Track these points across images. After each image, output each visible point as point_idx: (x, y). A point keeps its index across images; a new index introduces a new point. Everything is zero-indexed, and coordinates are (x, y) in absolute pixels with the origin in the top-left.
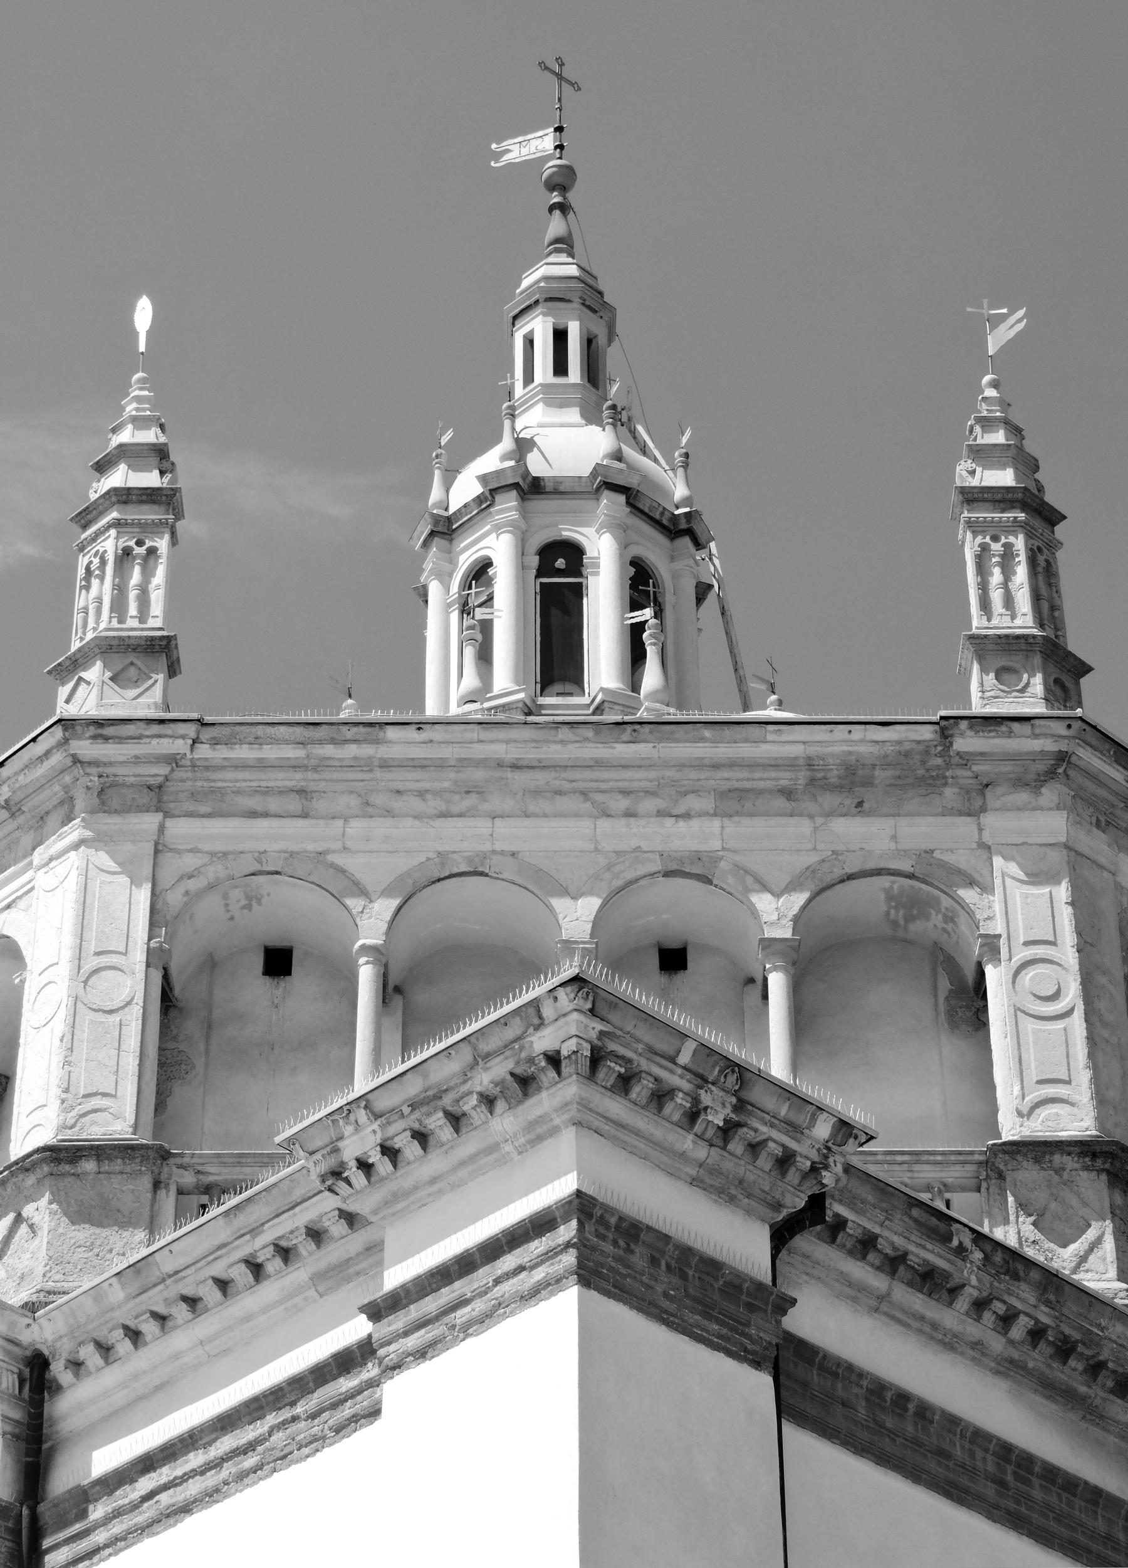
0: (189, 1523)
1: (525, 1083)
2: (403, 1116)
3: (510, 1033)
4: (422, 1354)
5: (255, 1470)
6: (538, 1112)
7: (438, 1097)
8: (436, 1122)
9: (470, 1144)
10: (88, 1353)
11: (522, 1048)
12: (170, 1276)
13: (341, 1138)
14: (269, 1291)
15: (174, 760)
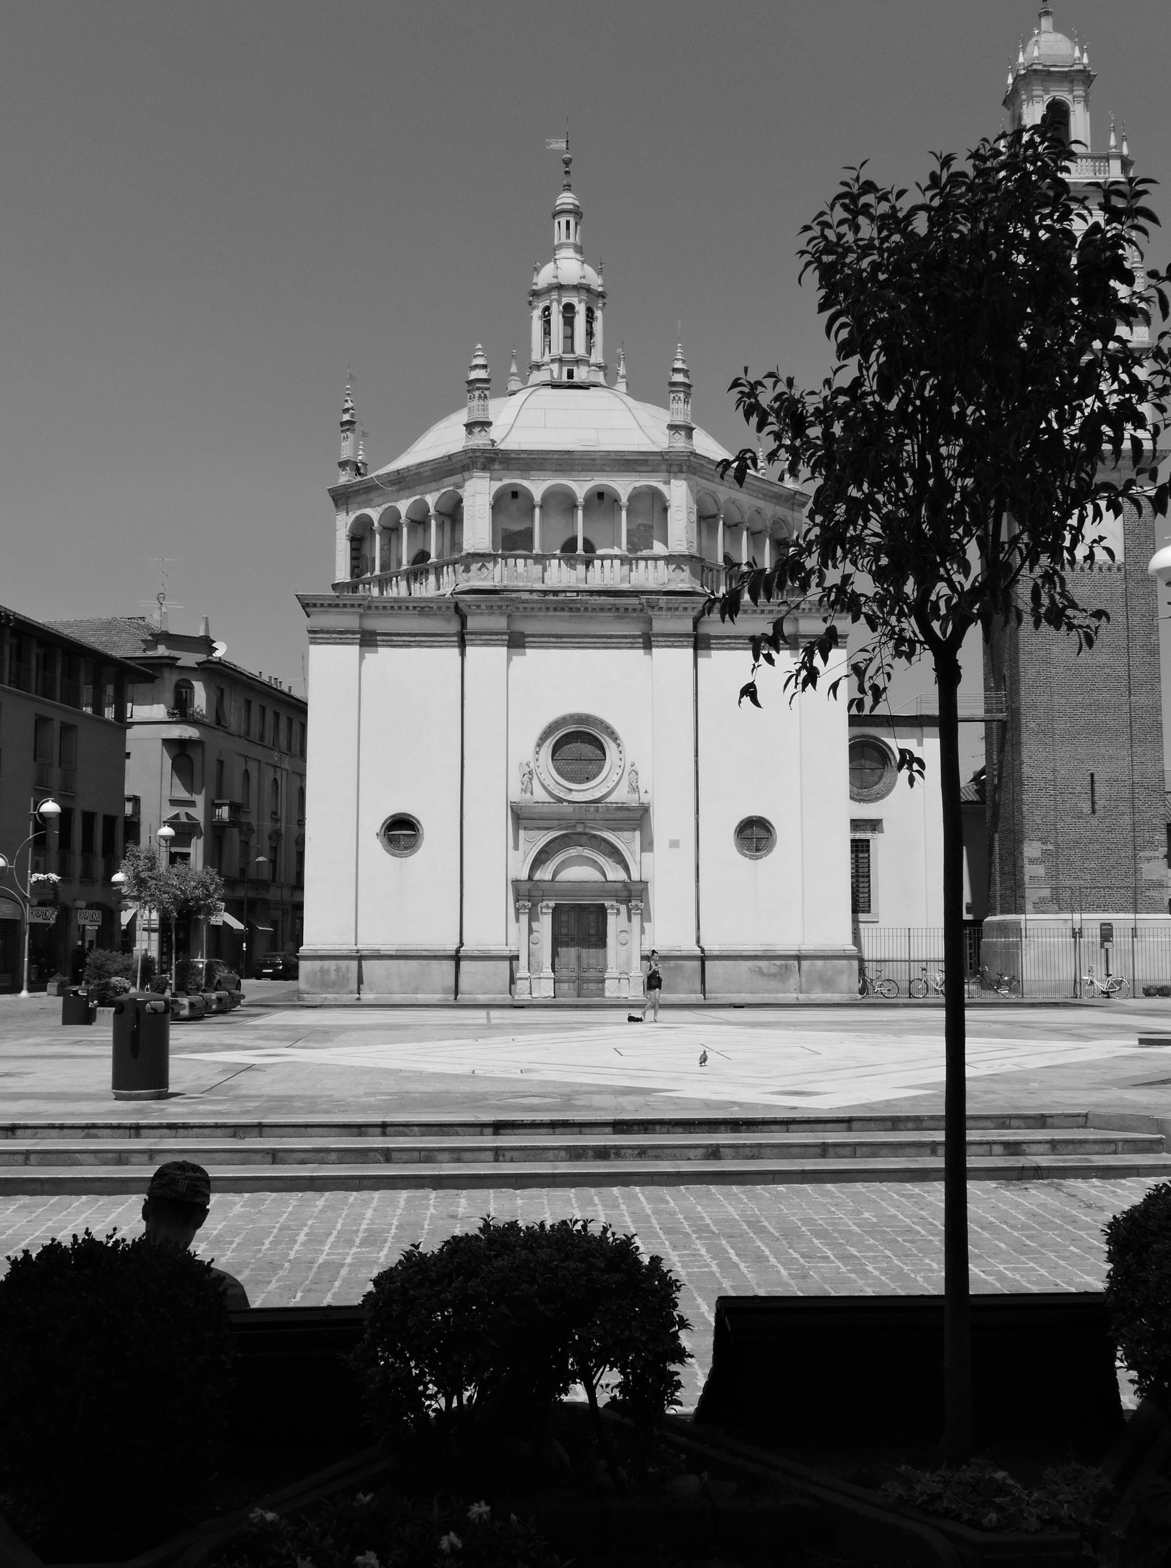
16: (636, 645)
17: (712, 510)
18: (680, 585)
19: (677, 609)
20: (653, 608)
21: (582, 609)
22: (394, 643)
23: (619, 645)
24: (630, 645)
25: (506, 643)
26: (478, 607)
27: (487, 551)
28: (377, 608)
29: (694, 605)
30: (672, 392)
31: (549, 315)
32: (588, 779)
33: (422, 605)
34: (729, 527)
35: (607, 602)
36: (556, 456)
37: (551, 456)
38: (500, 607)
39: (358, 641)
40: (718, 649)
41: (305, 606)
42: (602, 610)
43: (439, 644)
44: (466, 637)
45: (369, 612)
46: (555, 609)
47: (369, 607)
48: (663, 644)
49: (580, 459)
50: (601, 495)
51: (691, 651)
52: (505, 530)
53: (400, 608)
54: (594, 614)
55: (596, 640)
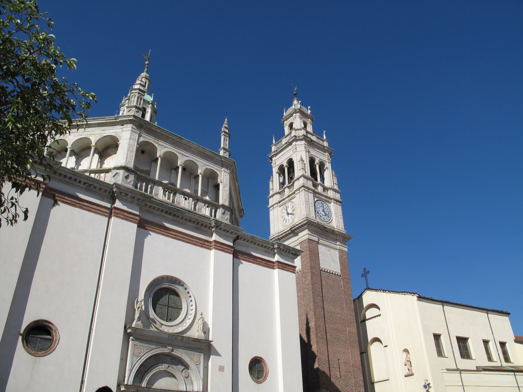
5: (258, 264)
14: (261, 248)
16: (204, 246)
19: (228, 231)
20: (217, 227)
24: (201, 245)
25: (137, 222)
26: (127, 195)
28: (60, 174)
29: (236, 232)
32: (171, 320)
33: (90, 183)
35: (194, 217)
36: (174, 138)
37: (172, 137)
42: (190, 221)
46: (166, 212)
49: (185, 145)
51: (232, 256)
53: (75, 180)
55: (184, 236)
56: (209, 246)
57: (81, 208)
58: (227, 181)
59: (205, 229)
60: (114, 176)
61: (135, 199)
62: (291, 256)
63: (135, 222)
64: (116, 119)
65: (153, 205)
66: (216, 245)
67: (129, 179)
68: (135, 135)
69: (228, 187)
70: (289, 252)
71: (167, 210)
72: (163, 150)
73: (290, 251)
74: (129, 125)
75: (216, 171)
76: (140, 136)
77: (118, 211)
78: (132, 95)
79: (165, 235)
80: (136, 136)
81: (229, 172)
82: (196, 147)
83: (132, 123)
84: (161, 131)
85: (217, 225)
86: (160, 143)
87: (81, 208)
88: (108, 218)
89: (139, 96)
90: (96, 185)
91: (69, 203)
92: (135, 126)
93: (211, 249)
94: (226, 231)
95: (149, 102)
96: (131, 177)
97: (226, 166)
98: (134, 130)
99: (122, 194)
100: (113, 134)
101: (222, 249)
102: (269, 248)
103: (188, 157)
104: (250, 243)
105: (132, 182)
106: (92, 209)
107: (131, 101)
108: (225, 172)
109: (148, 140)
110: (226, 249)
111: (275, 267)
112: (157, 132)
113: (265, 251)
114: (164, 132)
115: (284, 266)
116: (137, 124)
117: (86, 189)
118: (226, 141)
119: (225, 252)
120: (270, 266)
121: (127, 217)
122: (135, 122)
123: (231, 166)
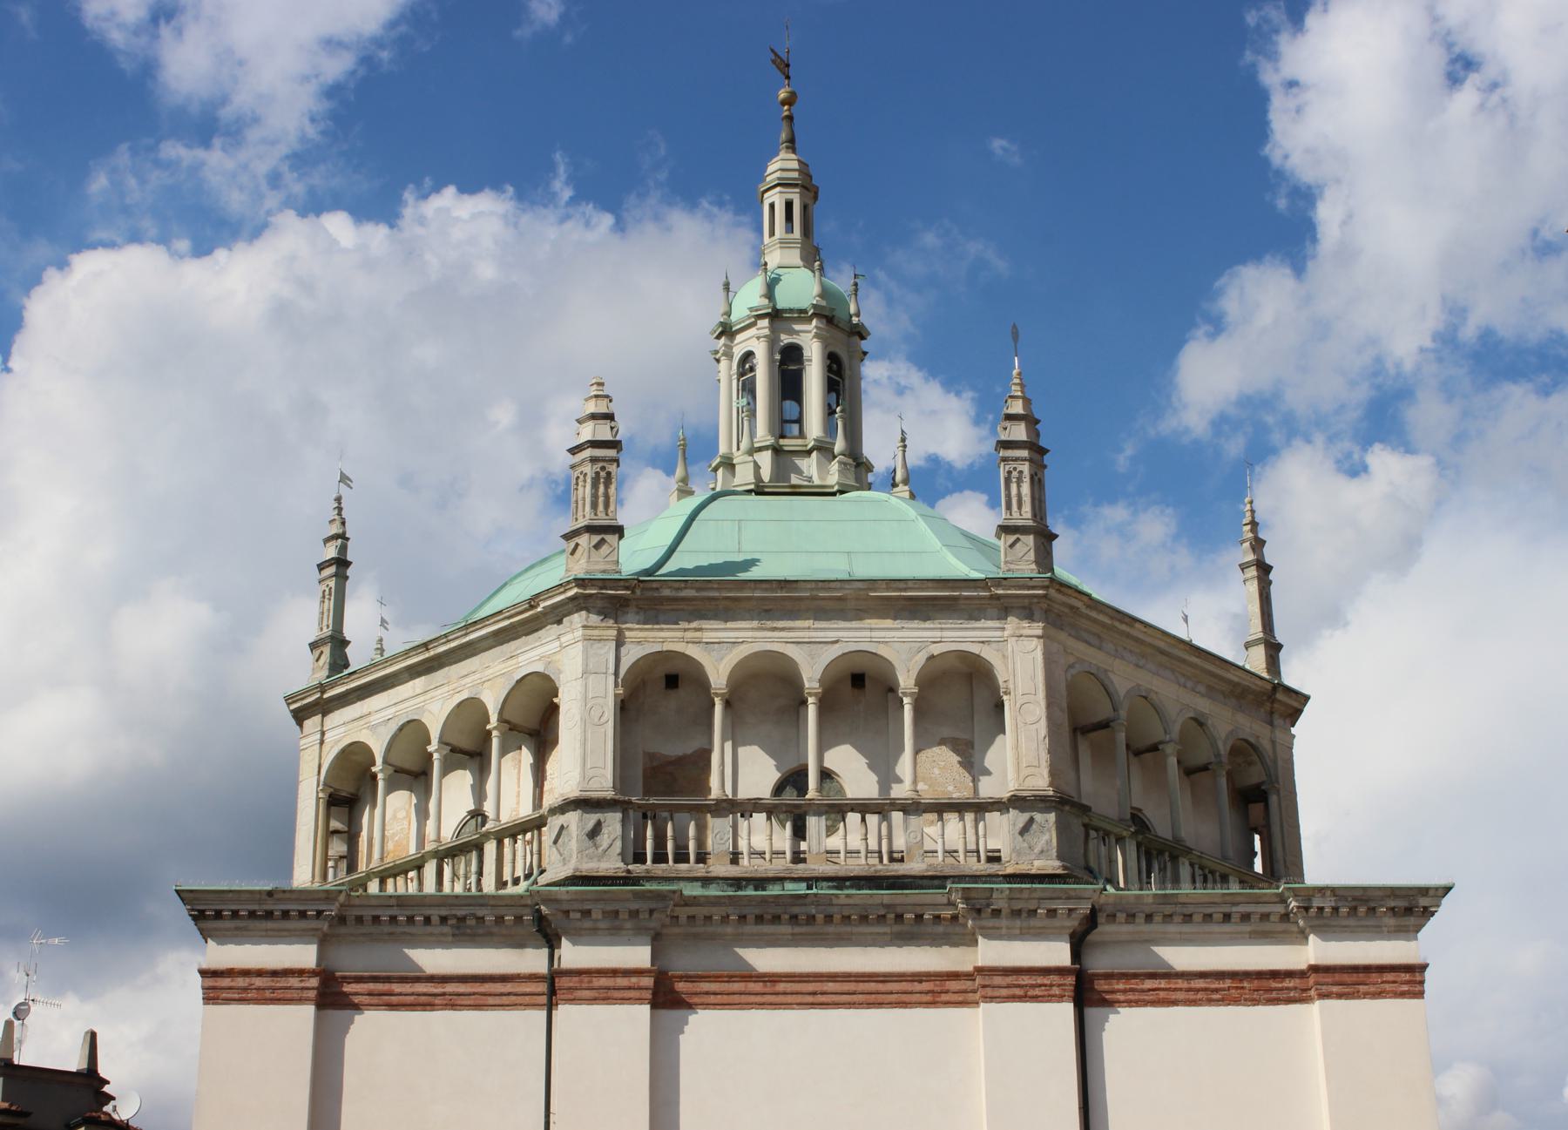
0: (1175, 1009)
1: (1409, 911)
2: (1347, 900)
3: (1411, 893)
4: (1340, 996)
5: (1218, 1000)
6: (1407, 923)
7: (1367, 901)
8: (1362, 910)
9: (1371, 922)
10: (1121, 917)
11: (1414, 899)
12: (1181, 904)
13: (1313, 896)
14: (1227, 928)
15: (1072, 607)
16: (944, 997)
17: (1103, 711)
18: (1037, 863)
20: (979, 911)
21: (820, 917)
22: (394, 999)
23: (905, 998)
24: (928, 998)
25: (648, 995)
27: (610, 794)
30: (1004, 459)
31: (752, 369)
33: (460, 912)
34: (1138, 753)
38: (634, 914)
39: (312, 994)
40: (1130, 1003)
41: (199, 917)
42: (864, 919)
43: (497, 1000)
44: (562, 982)
45: (343, 930)
46: (760, 919)
47: (342, 919)
48: (1004, 992)
50: (858, 680)
51: (1068, 1008)
52: (651, 756)
54: (848, 929)
56: (965, 992)
57: (453, 1005)
58: (1034, 678)
59: (940, 929)
60: (555, 842)
61: (621, 916)
62: (1390, 921)
63: (639, 1001)
64: (532, 607)
65: (700, 912)
66: (987, 983)
67: (606, 836)
68: (602, 652)
69: (1043, 704)
70: (1372, 910)
71: (758, 911)
72: (725, 661)
73: (1372, 905)
74: (576, 615)
75: (974, 649)
76: (620, 642)
77: (570, 981)
78: (576, 476)
79: (771, 1004)
80: (608, 652)
81: (1039, 632)
82: (860, 589)
83: (583, 605)
84: (698, 590)
85: (978, 907)
86: (708, 636)
87: (453, 1005)
88: (543, 1014)
89: (597, 474)
90: (480, 913)
91: (409, 1002)
92: (599, 613)
93: (977, 1003)
94: (1024, 915)
95: (804, 311)
96: (610, 828)
97: (1024, 608)
98: (596, 632)
99: (572, 915)
100: (539, 668)
101: (1018, 992)
102: (1265, 917)
103: (836, 642)
104: (1164, 922)
105: (618, 844)
106: (489, 998)
107: (577, 502)
108: (1021, 636)
109: (657, 648)
110: (1033, 986)
111: (1312, 993)
112: (684, 599)
113: (1250, 933)
114: (712, 589)
115: (1354, 977)
116: (599, 603)
117: (453, 935)
118: (1019, 481)
119: (1035, 999)
120: (1284, 995)
121: (608, 988)
122: (591, 601)
123: (1043, 600)
